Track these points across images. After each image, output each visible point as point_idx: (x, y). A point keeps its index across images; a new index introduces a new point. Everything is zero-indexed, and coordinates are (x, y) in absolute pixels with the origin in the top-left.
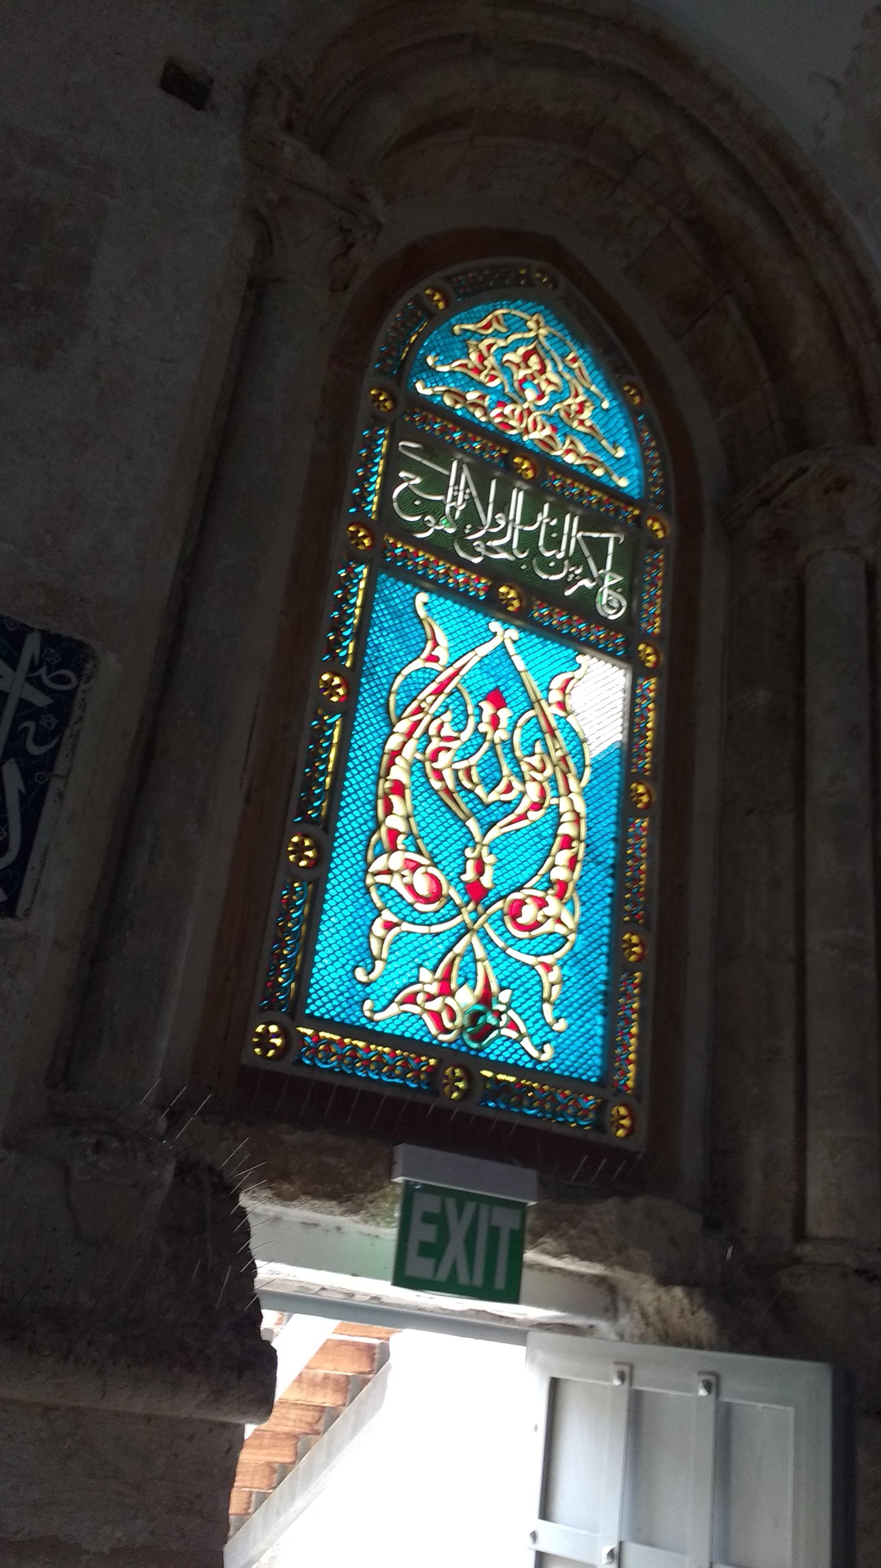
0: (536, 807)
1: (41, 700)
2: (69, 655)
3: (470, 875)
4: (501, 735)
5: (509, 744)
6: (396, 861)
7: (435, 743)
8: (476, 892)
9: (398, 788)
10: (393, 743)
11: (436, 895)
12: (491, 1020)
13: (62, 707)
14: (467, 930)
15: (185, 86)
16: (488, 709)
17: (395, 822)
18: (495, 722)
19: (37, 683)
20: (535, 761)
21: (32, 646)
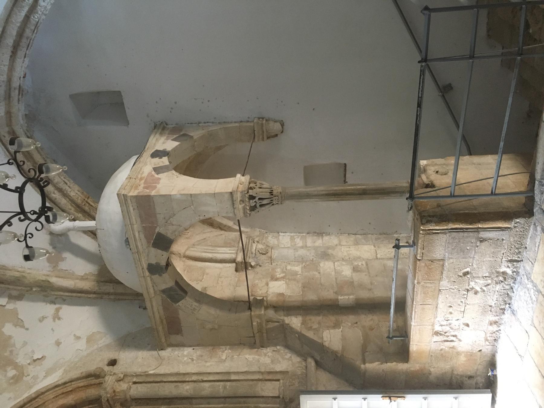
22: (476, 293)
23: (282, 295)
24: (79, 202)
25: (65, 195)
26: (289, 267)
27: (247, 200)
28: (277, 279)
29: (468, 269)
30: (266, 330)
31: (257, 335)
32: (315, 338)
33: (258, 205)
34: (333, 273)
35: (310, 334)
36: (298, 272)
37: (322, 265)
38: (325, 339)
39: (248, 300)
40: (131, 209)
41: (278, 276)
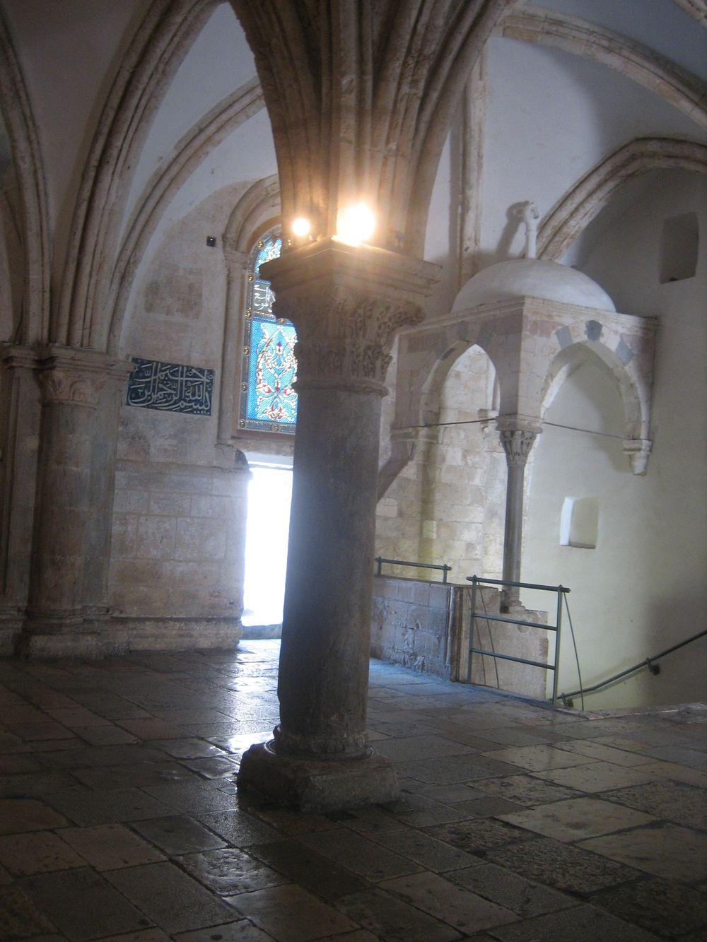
0: (289, 368)
1: (209, 381)
2: (211, 372)
3: (276, 385)
4: (281, 353)
5: (282, 355)
6: (261, 385)
7: (267, 358)
8: (277, 389)
9: (260, 370)
10: (259, 359)
11: (269, 391)
12: (281, 414)
13: (212, 381)
14: (275, 398)
15: (211, 242)
16: (278, 347)
17: (260, 377)
18: (279, 350)
19: (207, 378)
20: (288, 357)
21: (206, 372)
22: (404, 635)
23: (444, 460)
24: (565, 230)
25: (572, 215)
26: (479, 471)
27: (510, 429)
28: (464, 457)
29: (420, 628)
30: (406, 442)
31: (401, 432)
32: (389, 491)
33: (506, 439)
34: (467, 520)
35: (394, 485)
36: (473, 481)
37: (480, 509)
38: (387, 500)
39: (441, 422)
40: (512, 309)
41: (469, 458)
